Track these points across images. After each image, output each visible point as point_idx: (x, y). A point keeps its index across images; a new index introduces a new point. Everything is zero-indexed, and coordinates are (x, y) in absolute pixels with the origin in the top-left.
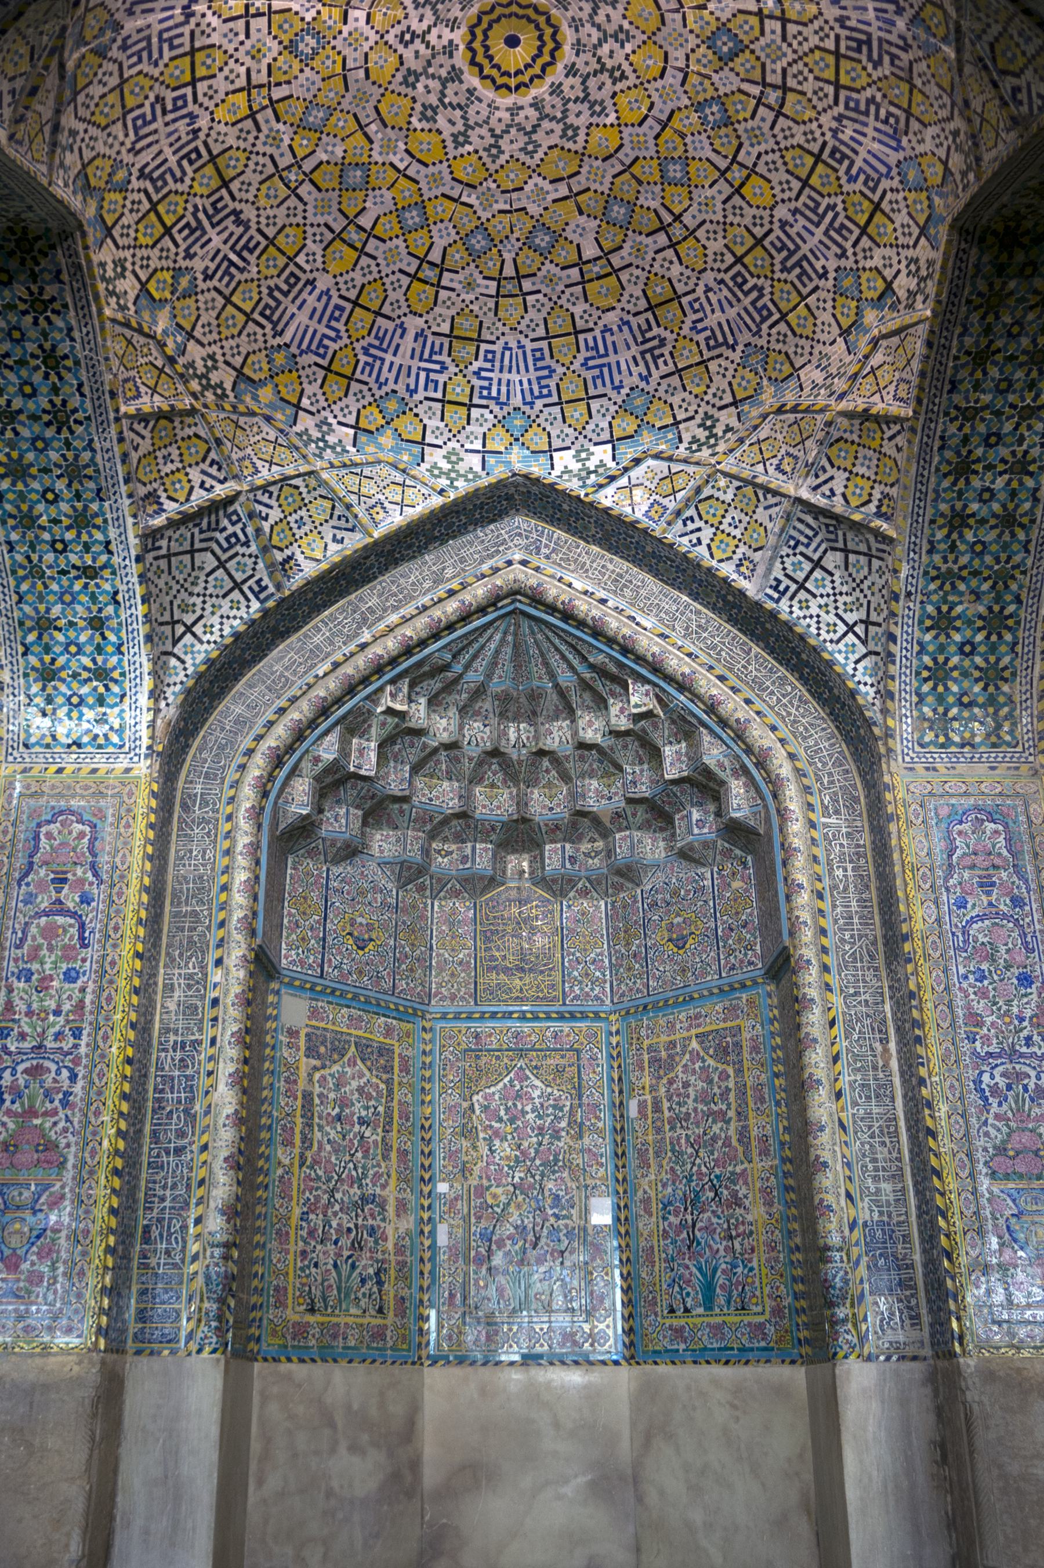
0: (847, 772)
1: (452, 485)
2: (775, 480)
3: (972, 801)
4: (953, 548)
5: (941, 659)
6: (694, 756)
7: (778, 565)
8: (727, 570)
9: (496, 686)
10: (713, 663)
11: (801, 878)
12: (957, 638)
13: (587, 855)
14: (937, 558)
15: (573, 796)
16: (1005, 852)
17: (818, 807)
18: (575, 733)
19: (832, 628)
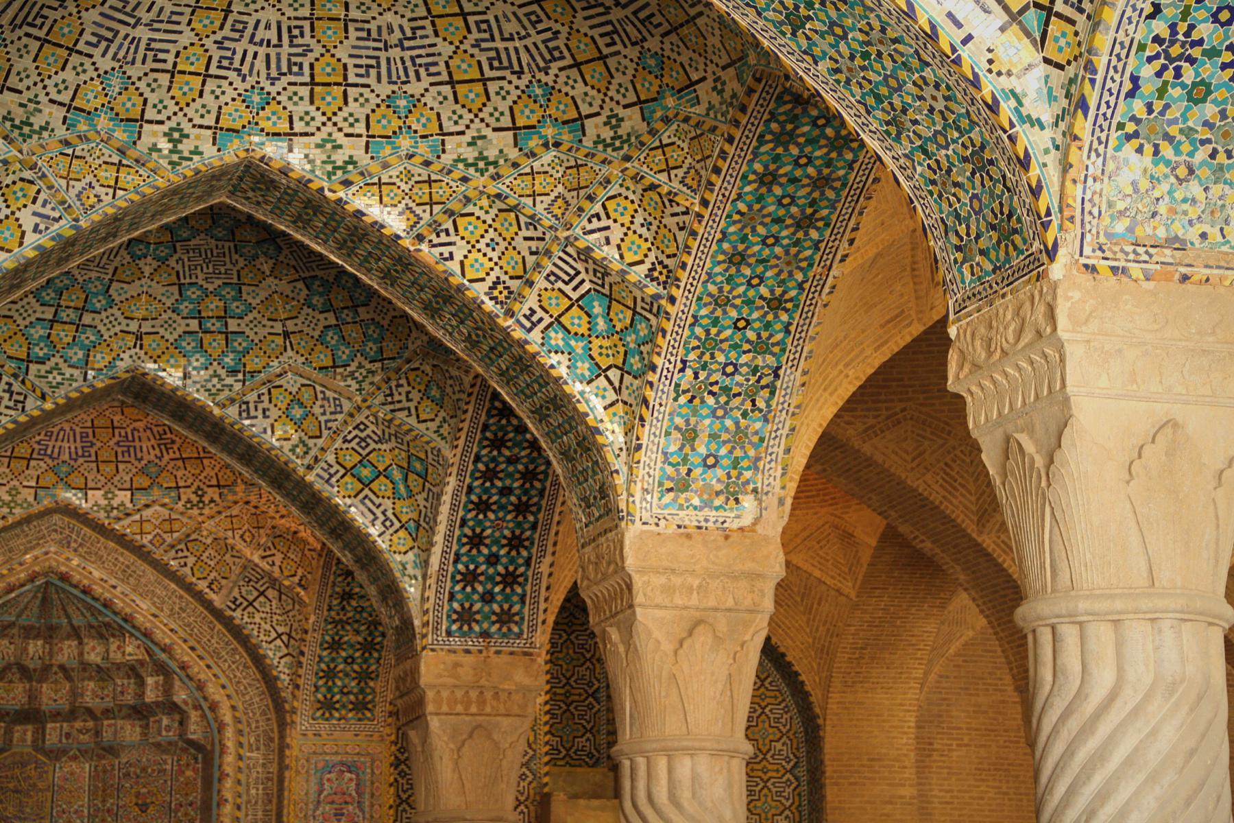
0: (268, 719)
1: (11, 513)
2: (240, 545)
3: (339, 758)
4: (343, 608)
5: (332, 666)
6: (168, 689)
7: (236, 589)
8: (202, 585)
9: (23, 621)
10: (188, 637)
11: (228, 795)
12: (344, 654)
13: (80, 731)
14: (333, 613)
15: (74, 694)
16: (354, 793)
17: (246, 745)
18: (81, 654)
19: (267, 633)
